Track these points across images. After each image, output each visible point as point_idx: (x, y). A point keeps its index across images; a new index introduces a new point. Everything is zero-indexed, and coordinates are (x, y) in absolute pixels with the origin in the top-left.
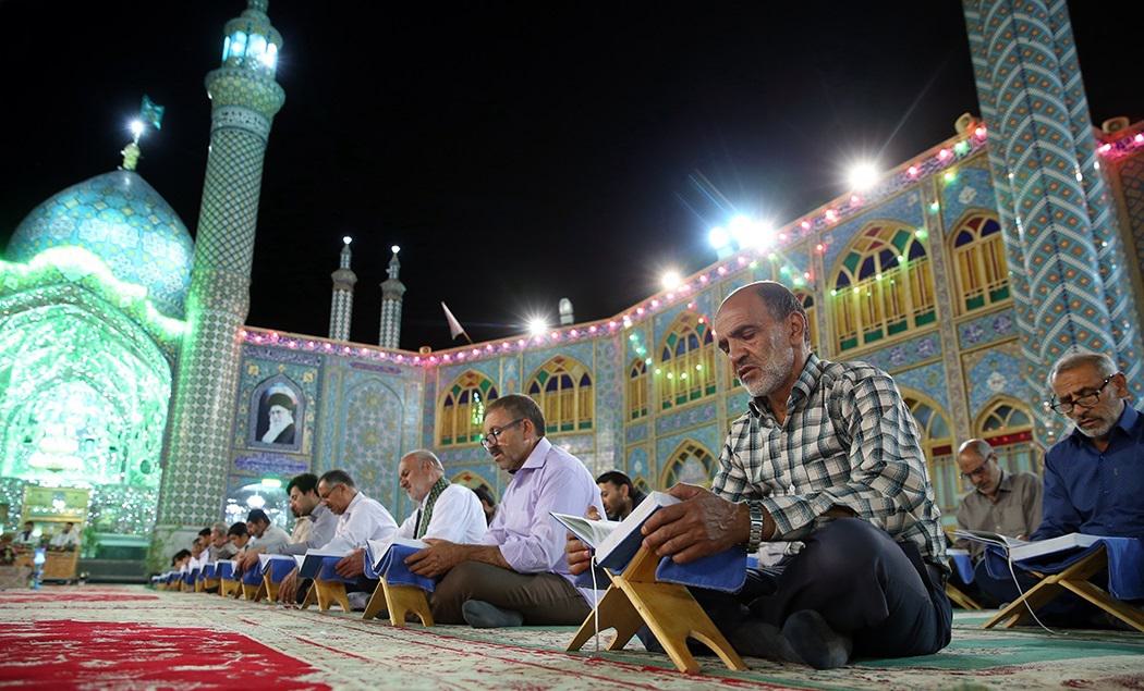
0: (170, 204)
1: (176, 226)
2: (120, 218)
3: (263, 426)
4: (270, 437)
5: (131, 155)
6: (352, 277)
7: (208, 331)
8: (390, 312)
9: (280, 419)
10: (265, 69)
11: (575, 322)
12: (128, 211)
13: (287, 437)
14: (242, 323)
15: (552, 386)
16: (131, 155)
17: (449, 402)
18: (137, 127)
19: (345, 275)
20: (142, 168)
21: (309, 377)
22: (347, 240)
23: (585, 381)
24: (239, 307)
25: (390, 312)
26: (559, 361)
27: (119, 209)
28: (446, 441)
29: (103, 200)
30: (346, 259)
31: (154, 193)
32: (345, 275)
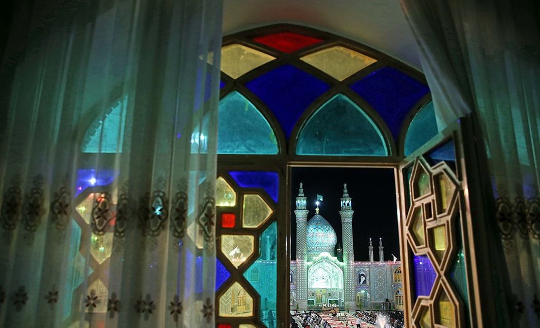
0: (332, 226)
3: (360, 281)
4: (361, 283)
5: (317, 210)
6: (372, 247)
7: (348, 264)
8: (381, 253)
9: (363, 279)
13: (365, 282)
16: (317, 210)
17: (395, 272)
18: (317, 203)
19: (371, 248)
20: (320, 213)
21: (367, 269)
24: (353, 258)
25: (381, 253)
32: (371, 248)
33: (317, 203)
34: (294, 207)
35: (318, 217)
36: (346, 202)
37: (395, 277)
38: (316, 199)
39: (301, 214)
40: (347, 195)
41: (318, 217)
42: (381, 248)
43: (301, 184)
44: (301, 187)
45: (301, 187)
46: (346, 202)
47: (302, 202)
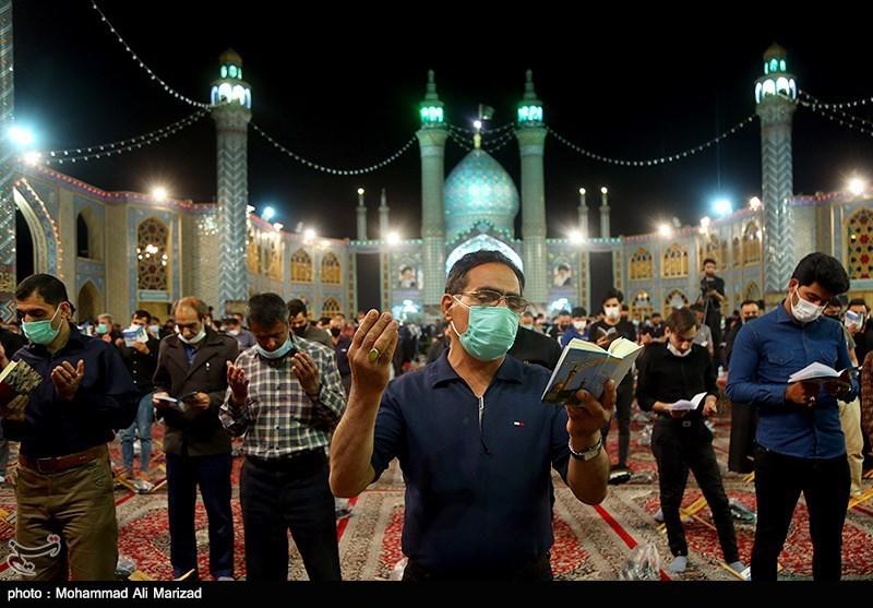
1: (505, 177)
2: (482, 182)
5: (477, 139)
10: (536, 121)
11: (682, 227)
12: (485, 177)
14: (544, 237)
15: (673, 255)
16: (477, 139)
17: (633, 260)
18: (477, 124)
20: (483, 147)
22: (582, 191)
23: (685, 254)
26: (676, 244)
27: (480, 177)
28: (633, 277)
29: (474, 174)
30: (583, 201)
31: (493, 161)
33: (477, 124)
34: (416, 124)
35: (478, 153)
36: (530, 113)
37: (633, 269)
38: (476, 117)
39: (430, 148)
40: (531, 95)
41: (478, 153)
42: (605, 207)
43: (431, 73)
44: (431, 78)
45: (431, 78)
46: (530, 113)
47: (432, 113)
